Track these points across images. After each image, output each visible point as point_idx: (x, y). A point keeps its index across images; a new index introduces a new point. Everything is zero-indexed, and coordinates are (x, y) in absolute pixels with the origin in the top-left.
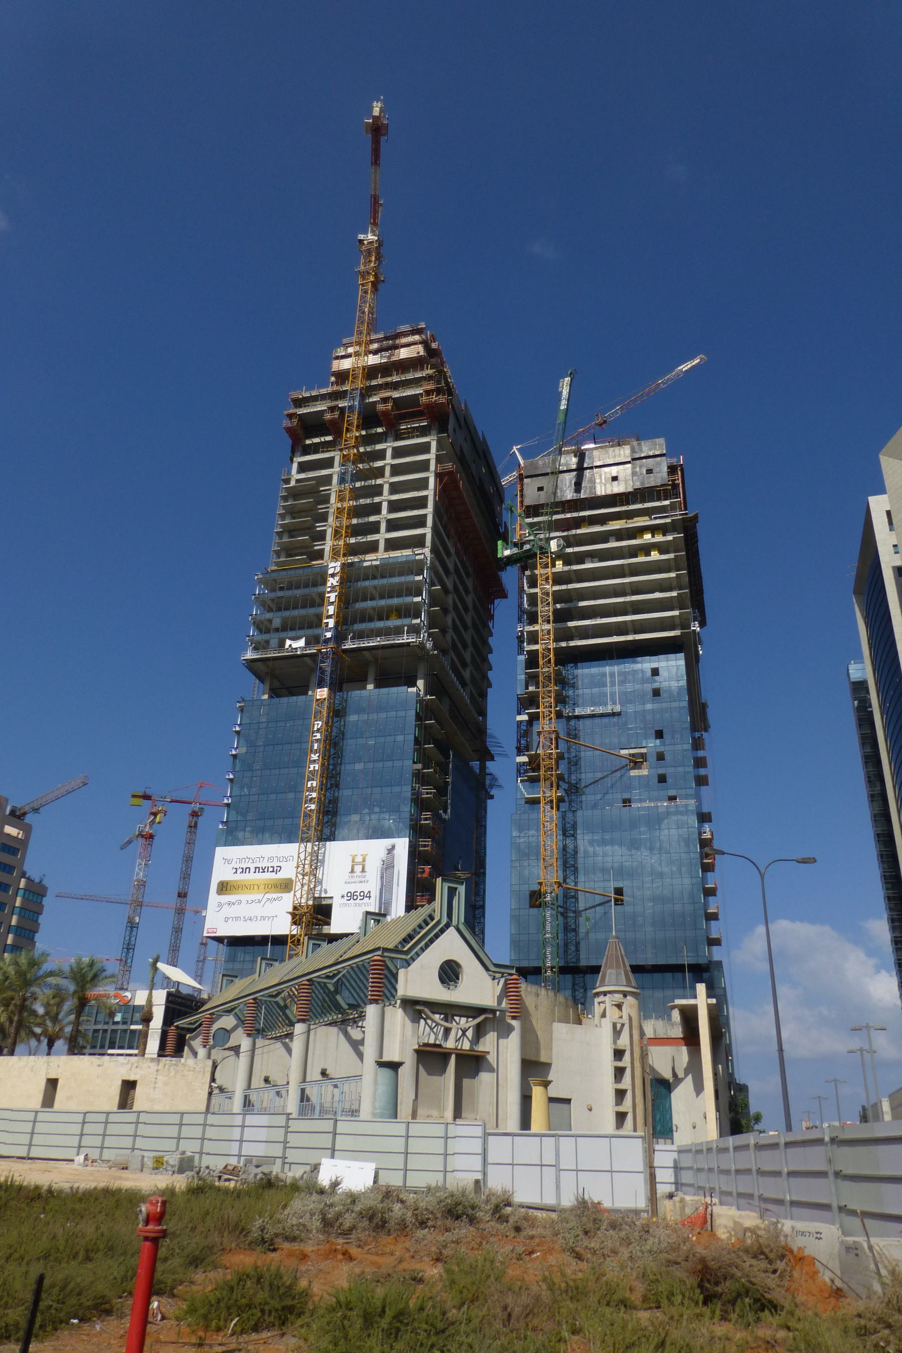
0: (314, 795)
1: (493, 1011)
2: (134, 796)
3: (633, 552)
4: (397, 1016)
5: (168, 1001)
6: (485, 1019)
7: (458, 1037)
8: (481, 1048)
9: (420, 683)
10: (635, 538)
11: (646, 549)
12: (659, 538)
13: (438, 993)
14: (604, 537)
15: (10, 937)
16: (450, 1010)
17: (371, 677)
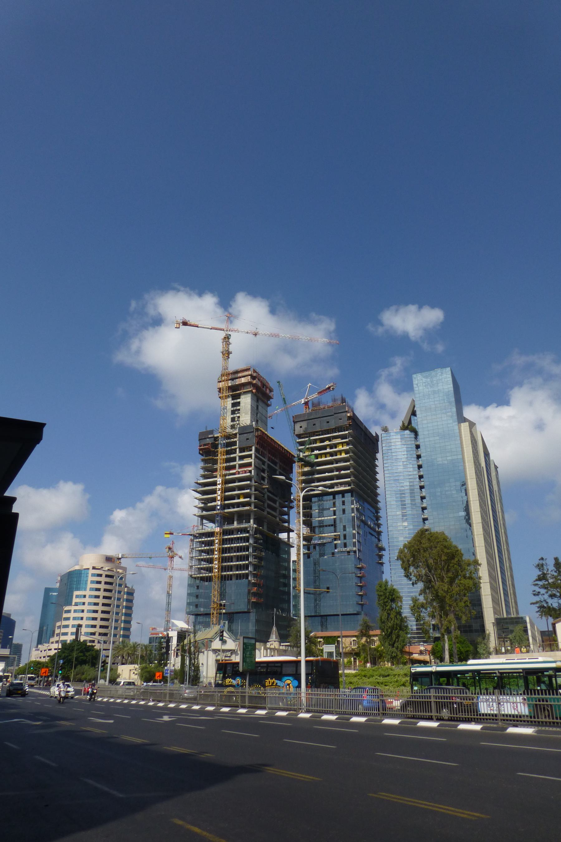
0: (217, 566)
1: (234, 650)
2: (166, 534)
3: (335, 454)
4: (211, 653)
5: (178, 635)
6: (233, 652)
9: (252, 521)
11: (340, 452)
12: (346, 447)
14: (325, 448)
15: (124, 610)
16: (224, 651)
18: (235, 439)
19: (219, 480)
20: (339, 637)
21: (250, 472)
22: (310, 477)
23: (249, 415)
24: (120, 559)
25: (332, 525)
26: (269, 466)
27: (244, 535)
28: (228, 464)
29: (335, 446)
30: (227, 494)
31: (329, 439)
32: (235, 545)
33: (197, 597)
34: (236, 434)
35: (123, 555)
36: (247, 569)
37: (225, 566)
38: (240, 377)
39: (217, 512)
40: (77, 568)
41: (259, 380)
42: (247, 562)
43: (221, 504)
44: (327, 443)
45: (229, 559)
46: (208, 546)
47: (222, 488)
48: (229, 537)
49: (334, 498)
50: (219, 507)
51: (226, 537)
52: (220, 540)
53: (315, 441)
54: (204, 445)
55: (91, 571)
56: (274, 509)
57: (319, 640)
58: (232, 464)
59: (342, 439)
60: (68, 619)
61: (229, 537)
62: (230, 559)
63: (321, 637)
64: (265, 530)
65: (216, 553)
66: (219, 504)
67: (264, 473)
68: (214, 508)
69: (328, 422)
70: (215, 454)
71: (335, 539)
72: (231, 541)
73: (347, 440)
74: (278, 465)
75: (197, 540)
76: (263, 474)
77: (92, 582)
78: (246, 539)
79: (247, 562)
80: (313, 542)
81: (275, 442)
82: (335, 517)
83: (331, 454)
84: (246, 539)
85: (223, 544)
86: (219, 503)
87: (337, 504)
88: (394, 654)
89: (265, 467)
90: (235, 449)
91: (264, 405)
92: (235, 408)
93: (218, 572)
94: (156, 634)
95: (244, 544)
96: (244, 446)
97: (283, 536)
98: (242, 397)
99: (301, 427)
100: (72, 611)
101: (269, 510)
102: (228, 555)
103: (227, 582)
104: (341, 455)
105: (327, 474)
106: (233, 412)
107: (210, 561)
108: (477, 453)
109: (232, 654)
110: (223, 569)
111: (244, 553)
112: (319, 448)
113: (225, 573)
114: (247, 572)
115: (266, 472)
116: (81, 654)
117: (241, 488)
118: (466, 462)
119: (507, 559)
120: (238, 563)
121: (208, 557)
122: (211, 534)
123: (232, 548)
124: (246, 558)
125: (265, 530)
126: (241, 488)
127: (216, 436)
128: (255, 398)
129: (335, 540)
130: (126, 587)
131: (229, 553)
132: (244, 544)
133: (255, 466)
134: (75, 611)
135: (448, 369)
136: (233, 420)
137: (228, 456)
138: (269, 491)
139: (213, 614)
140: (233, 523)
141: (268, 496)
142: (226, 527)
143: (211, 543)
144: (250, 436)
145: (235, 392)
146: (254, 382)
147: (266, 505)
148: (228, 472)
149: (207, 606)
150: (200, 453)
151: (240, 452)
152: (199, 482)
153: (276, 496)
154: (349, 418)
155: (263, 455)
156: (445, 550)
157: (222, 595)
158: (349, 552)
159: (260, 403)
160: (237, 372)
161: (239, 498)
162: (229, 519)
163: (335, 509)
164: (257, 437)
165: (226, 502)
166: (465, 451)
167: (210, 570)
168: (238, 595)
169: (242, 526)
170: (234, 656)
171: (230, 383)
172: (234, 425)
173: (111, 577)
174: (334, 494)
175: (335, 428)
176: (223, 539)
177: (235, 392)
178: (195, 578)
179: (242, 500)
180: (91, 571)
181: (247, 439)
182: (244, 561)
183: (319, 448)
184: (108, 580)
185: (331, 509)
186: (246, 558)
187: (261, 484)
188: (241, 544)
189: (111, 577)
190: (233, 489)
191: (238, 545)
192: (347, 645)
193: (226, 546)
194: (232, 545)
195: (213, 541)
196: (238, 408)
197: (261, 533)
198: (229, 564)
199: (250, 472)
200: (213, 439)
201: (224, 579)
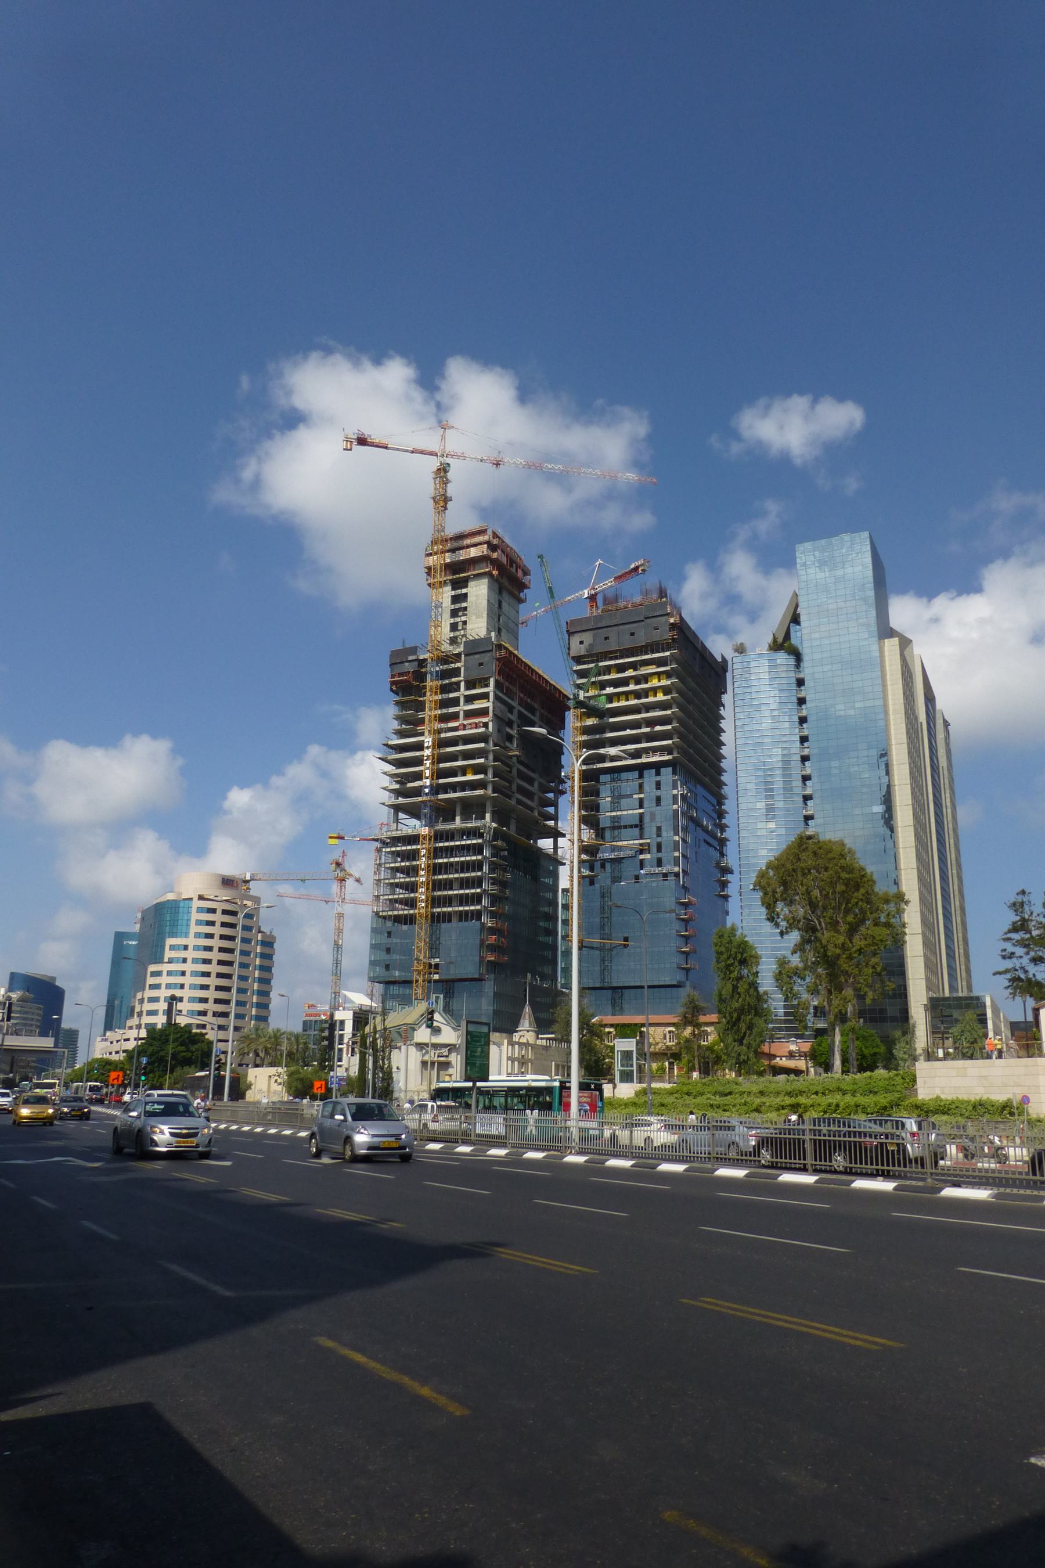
0: (423, 897)
1: (455, 1045)
3: (645, 693)
4: (412, 1050)
6: (452, 1048)
8: (449, 1059)
9: (488, 816)
10: (646, 683)
11: (655, 690)
12: (665, 682)
14: (625, 682)
15: (257, 972)
16: (435, 1046)
17: (458, 810)
18: (458, 665)
19: (428, 740)
20: (643, 1025)
21: (486, 725)
22: (597, 736)
23: (485, 619)
24: (248, 882)
25: (636, 826)
26: (521, 715)
27: (474, 842)
28: (444, 711)
29: (646, 678)
30: (442, 765)
31: (634, 666)
32: (457, 859)
33: (388, 950)
34: (458, 655)
35: (252, 875)
36: (479, 902)
37: (439, 896)
38: (468, 547)
39: (425, 798)
40: (171, 896)
41: (503, 552)
42: (479, 890)
43: (431, 785)
44: (630, 673)
45: (445, 884)
46: (408, 860)
47: (433, 755)
48: (446, 844)
49: (641, 776)
50: (427, 790)
51: (441, 845)
52: (429, 850)
53: (608, 670)
54: (400, 674)
55: (197, 904)
56: (530, 795)
57: (607, 1030)
58: (451, 710)
59: (659, 666)
60: (157, 987)
61: (446, 844)
62: (448, 885)
63: (612, 1026)
64: (513, 831)
65: (422, 873)
66: (428, 784)
67: (512, 728)
68: (418, 792)
69: (632, 634)
70: (421, 691)
71: (641, 852)
72: (450, 851)
73: (668, 668)
74: (538, 714)
75: (388, 850)
76: (509, 730)
77: (199, 923)
78: (478, 849)
79: (479, 890)
80: (600, 855)
81: (533, 670)
82: (641, 811)
83: (638, 695)
84: (478, 849)
85: (435, 858)
86: (428, 782)
87: (646, 787)
88: (742, 1057)
89: (514, 717)
90: (458, 683)
91: (513, 601)
92: (457, 606)
93: (427, 907)
94: (316, 1015)
95: (474, 858)
96: (474, 676)
97: (546, 844)
98: (471, 584)
99: (581, 643)
100: (165, 973)
101: (520, 797)
102: (445, 876)
103: (443, 926)
104: (655, 695)
105: (628, 732)
106: (454, 613)
107: (412, 887)
108: (912, 696)
109: (450, 1051)
110: (435, 902)
111: (473, 874)
112: (615, 683)
113: (439, 910)
114: (478, 907)
115: (515, 726)
116: (183, 1048)
117: (468, 755)
118: (891, 712)
119: (957, 893)
120: (462, 892)
121: (407, 880)
122: (413, 839)
123: (451, 864)
124: (478, 882)
125: (513, 831)
126: (468, 755)
127: (421, 657)
128: (496, 585)
129: (641, 853)
130: (260, 932)
131: (446, 873)
132: (474, 858)
133: (494, 715)
134: (170, 973)
135: (866, 534)
136: (454, 627)
137: (445, 696)
138: (520, 762)
139: (417, 981)
140: (454, 820)
141: (518, 770)
142: (441, 827)
143: (414, 855)
144: (486, 658)
145: (458, 574)
146: (495, 555)
147: (514, 787)
148: (443, 726)
149: (406, 967)
150: (391, 690)
151: (467, 688)
152: (390, 743)
153: (533, 771)
154: (673, 626)
155: (509, 693)
156: (844, 875)
157: (434, 948)
158: (665, 875)
159: (506, 596)
160: (461, 537)
161: (464, 774)
162: (446, 812)
163: (642, 796)
164: (498, 660)
165: (441, 781)
166: (890, 692)
167: (412, 903)
168: (463, 948)
169: (469, 825)
170: (453, 1055)
171: (448, 558)
172: (456, 637)
173: (234, 913)
174: (641, 769)
175: (646, 646)
176: (435, 849)
177: (458, 574)
178: (384, 918)
179: (470, 777)
180: (197, 904)
181: (481, 664)
182: (473, 888)
183: (615, 683)
184: (228, 919)
185: (635, 796)
186: (478, 882)
187: (505, 748)
188: (468, 858)
189: (234, 913)
190: (453, 757)
191: (463, 859)
192: (658, 1040)
193: (441, 861)
194: (452, 860)
195: (417, 851)
196: (464, 605)
197: (505, 837)
198: (445, 893)
199: (486, 725)
200: (416, 663)
201: (436, 919)
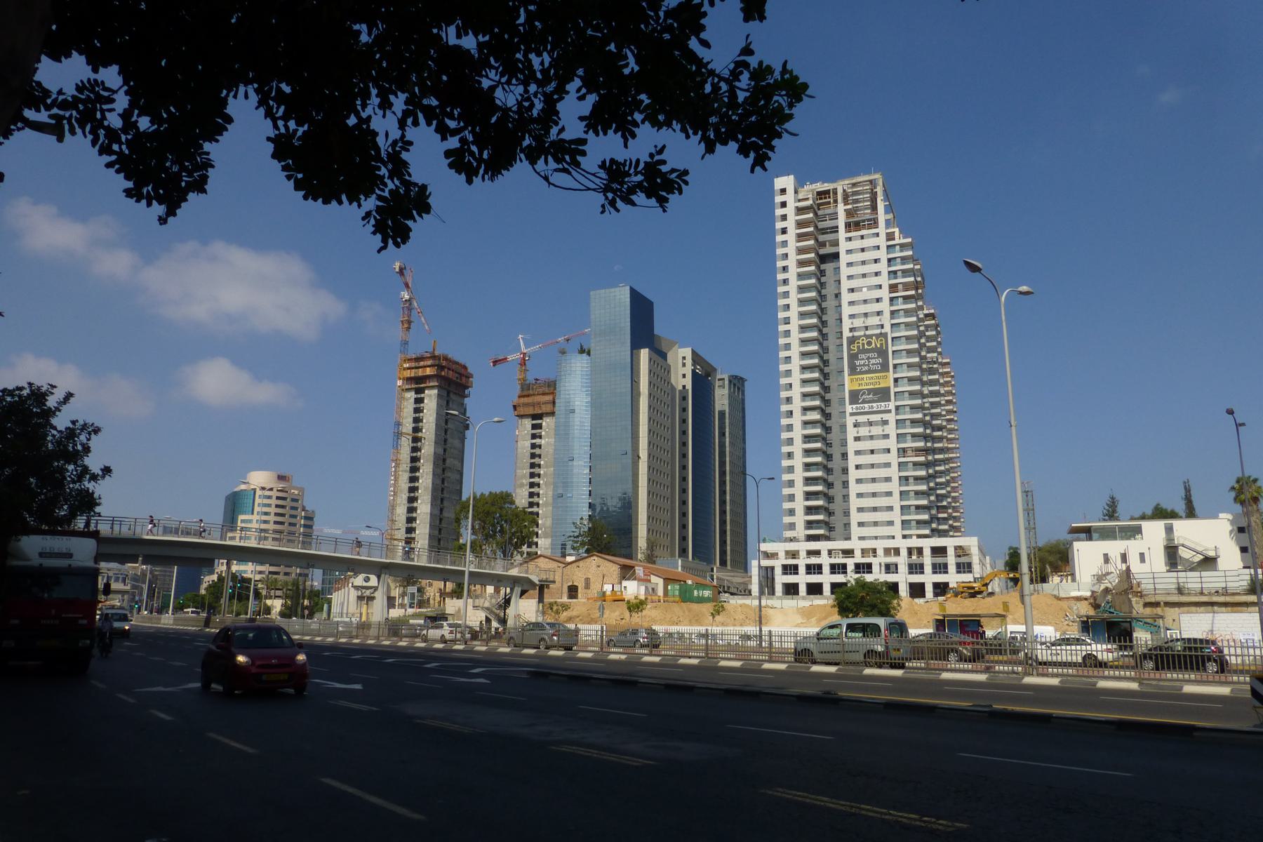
4: (352, 590)
6: (376, 589)
7: (368, 593)
13: (365, 584)
40: (243, 487)
173: (284, 499)
184: (280, 502)
189: (284, 499)
